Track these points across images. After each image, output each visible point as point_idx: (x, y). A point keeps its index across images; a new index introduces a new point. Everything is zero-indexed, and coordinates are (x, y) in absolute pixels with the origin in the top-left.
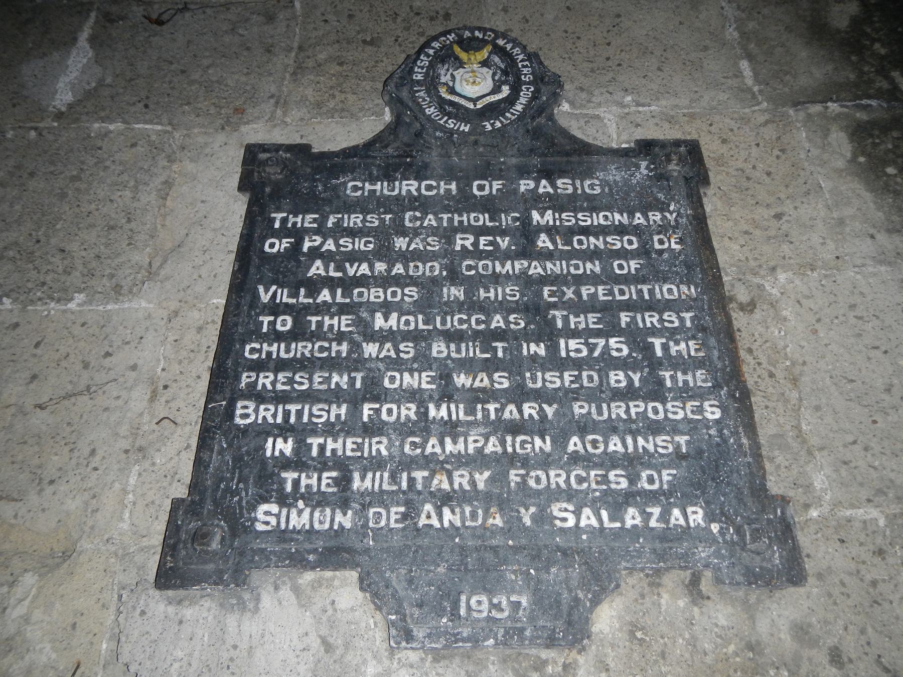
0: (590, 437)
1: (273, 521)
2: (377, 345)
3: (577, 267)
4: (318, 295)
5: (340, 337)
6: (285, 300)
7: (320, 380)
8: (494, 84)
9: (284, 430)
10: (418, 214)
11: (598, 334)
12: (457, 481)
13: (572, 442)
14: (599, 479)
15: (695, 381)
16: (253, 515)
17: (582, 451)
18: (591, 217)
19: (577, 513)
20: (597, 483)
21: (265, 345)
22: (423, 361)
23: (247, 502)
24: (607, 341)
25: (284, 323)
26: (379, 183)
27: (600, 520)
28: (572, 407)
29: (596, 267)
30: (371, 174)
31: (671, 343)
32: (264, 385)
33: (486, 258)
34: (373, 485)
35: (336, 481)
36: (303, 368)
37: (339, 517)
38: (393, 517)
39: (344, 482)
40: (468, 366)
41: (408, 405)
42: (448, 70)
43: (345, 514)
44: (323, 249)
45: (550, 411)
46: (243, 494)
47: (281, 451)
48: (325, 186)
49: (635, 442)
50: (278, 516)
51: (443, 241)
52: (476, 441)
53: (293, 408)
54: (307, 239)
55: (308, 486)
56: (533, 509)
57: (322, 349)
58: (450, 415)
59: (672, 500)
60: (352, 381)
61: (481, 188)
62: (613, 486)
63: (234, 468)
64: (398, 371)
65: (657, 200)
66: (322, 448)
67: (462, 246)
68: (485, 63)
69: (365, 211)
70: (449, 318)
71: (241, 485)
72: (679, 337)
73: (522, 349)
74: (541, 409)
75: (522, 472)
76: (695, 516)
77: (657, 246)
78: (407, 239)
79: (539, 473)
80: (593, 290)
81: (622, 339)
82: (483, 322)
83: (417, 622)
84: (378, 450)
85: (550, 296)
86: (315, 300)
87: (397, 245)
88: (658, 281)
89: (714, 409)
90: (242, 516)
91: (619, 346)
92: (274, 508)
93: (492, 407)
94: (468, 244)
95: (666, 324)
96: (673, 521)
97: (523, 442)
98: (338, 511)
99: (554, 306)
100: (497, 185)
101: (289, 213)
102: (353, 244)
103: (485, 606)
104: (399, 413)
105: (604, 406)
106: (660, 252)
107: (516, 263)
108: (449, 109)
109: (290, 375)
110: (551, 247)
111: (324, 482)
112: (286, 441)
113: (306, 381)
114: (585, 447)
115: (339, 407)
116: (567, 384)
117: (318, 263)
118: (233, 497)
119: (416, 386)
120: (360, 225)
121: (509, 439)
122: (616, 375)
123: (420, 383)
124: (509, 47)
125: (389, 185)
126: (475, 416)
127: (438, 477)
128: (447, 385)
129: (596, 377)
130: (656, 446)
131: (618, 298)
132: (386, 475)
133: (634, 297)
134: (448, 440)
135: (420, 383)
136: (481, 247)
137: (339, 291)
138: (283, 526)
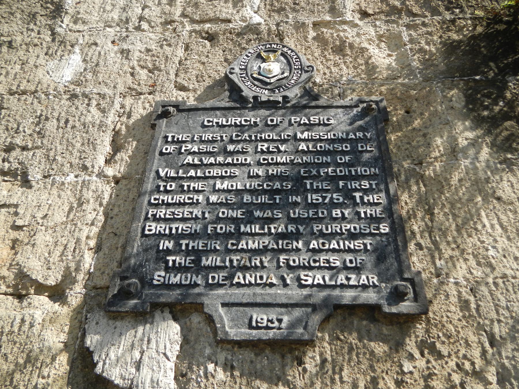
1: (162, 280)
2: (217, 196)
3: (318, 159)
5: (198, 192)
9: (170, 236)
11: (327, 191)
17: (317, 248)
20: (324, 263)
25: (171, 186)
30: (216, 115)
32: (160, 216)
37: (194, 277)
39: (197, 261)
40: (262, 206)
45: (301, 228)
47: (167, 247)
49: (344, 244)
53: (174, 226)
55: (180, 264)
57: (189, 198)
66: (187, 245)
67: (261, 149)
68: (278, 61)
69: (213, 133)
71: (147, 263)
74: (297, 227)
77: (360, 149)
85: (304, 173)
87: (229, 150)
88: (359, 166)
91: (338, 197)
92: (163, 274)
93: (272, 226)
95: (363, 187)
97: (287, 243)
98: (194, 275)
99: (306, 178)
102: (207, 148)
103: (265, 321)
104: (226, 230)
111: (188, 261)
112: (170, 242)
116: (310, 216)
119: (235, 216)
121: (280, 242)
124: (289, 52)
130: (354, 245)
132: (219, 259)
133: (347, 174)
138: (167, 282)
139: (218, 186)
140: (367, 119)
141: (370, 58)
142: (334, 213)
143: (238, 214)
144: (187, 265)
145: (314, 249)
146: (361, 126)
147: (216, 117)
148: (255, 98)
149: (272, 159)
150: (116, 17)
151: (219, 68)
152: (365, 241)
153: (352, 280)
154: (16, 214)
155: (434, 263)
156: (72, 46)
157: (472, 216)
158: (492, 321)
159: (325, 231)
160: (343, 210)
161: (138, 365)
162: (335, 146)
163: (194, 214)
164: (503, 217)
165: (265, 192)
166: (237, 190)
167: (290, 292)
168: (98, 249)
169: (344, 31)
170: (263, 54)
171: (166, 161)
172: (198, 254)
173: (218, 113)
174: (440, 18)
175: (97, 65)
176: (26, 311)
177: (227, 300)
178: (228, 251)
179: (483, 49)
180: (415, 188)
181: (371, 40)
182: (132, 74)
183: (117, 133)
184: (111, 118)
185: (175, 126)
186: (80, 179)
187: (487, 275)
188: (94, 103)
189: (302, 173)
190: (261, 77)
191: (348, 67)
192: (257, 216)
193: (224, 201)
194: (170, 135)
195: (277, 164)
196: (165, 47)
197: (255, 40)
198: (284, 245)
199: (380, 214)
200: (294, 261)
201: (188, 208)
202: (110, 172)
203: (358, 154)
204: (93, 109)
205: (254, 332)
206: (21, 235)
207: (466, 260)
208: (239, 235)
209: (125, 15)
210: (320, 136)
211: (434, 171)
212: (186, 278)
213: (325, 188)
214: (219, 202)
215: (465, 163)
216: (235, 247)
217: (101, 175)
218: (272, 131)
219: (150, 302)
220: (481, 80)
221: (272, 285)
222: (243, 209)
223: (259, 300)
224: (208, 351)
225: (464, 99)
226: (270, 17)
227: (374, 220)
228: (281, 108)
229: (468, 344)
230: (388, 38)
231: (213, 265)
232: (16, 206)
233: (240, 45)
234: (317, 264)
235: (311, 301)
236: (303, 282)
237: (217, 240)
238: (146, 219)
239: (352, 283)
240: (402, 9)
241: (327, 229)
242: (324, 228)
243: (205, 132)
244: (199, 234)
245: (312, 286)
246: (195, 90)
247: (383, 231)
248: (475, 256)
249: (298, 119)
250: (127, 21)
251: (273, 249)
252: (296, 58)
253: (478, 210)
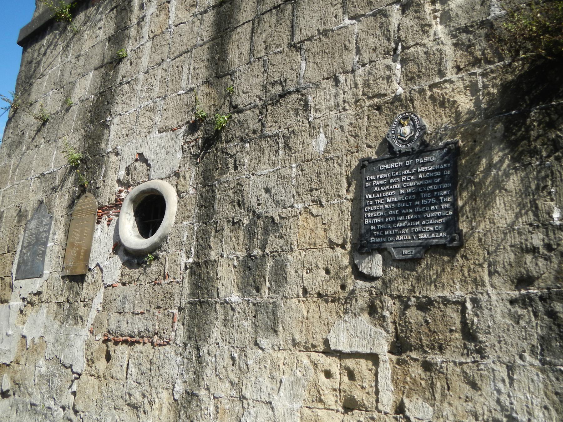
5: (381, 204)
11: (430, 198)
22: (397, 208)
29: (430, 181)
35: (382, 233)
39: (384, 233)
40: (405, 208)
45: (419, 216)
53: (374, 220)
68: (409, 124)
69: (384, 173)
92: (373, 238)
99: (421, 192)
108: (400, 141)
139: (388, 200)
140: (450, 155)
141: (458, 107)
143: (396, 212)
146: (446, 160)
147: (385, 164)
148: (400, 151)
150: (333, 104)
151: (385, 129)
154: (322, 219)
155: (472, 224)
156: (319, 128)
157: (492, 200)
158: (489, 246)
161: (371, 268)
164: (506, 199)
165: (405, 201)
166: (395, 202)
168: (351, 230)
169: (446, 88)
170: (402, 121)
172: (383, 230)
173: (385, 162)
174: (502, 63)
175: (332, 139)
176: (335, 253)
177: (394, 246)
178: (394, 228)
179: (524, 85)
180: (470, 188)
181: (460, 91)
182: (347, 141)
183: (348, 176)
184: (344, 168)
186: (339, 201)
187: (492, 228)
188: (335, 161)
190: (401, 137)
191: (446, 117)
194: (367, 177)
195: (410, 187)
196: (359, 120)
197: (400, 106)
202: (349, 197)
204: (336, 165)
206: (326, 227)
207: (485, 221)
208: (397, 222)
209: (336, 101)
211: (479, 178)
215: (494, 172)
217: (346, 199)
218: (407, 169)
220: (515, 113)
221: (409, 240)
223: (405, 245)
224: (390, 263)
225: (503, 129)
226: (406, 85)
227: (447, 209)
228: (411, 155)
229: (479, 255)
230: (470, 87)
232: (321, 215)
233: (393, 111)
235: (422, 244)
238: (365, 218)
240: (481, 59)
243: (381, 174)
245: (423, 239)
246: (375, 147)
248: (489, 219)
250: (338, 106)
253: (495, 197)
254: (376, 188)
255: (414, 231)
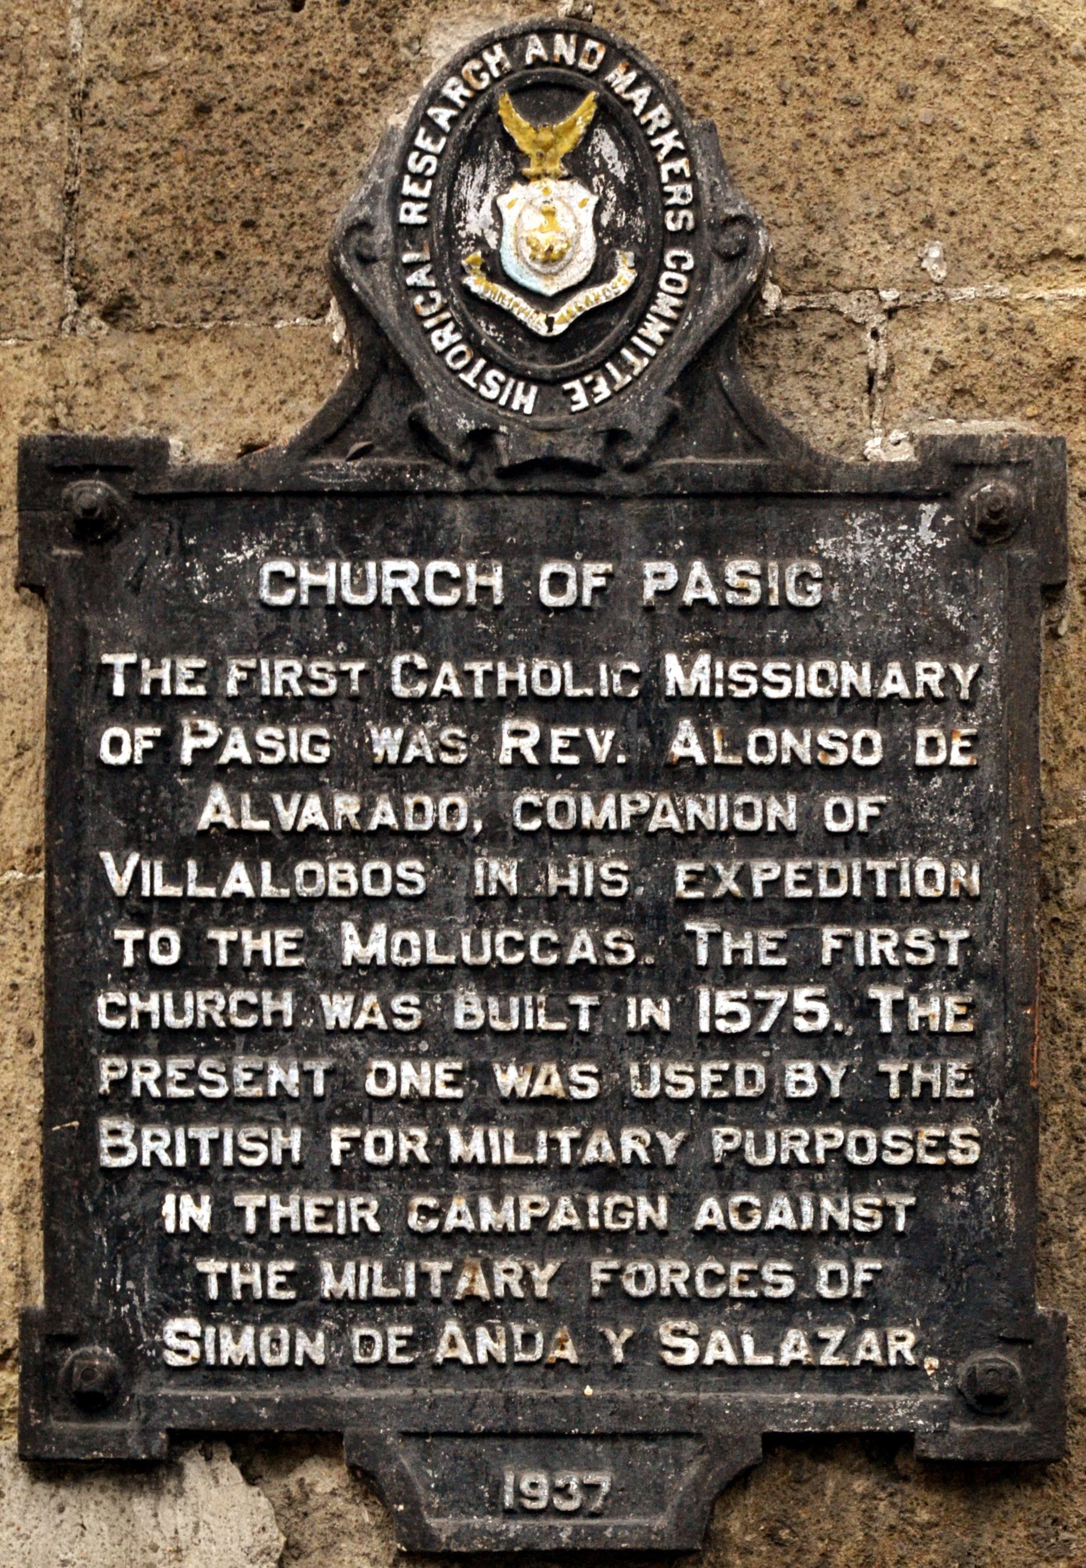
0: (737, 1199)
1: (195, 1350)
3: (748, 810)
4: (225, 878)
6: (159, 891)
7: (248, 1076)
8: (599, 240)
10: (421, 663)
11: (774, 976)
12: (500, 1279)
13: (704, 1210)
14: (746, 1278)
15: (944, 1086)
16: (157, 1338)
17: (722, 1227)
18: (791, 674)
19: (702, 1338)
20: (742, 1285)
21: (134, 998)
23: (144, 1315)
24: (790, 996)
26: (332, 566)
27: (739, 1351)
28: (711, 1139)
31: (913, 1001)
33: (562, 786)
34: (357, 1288)
35: (291, 1279)
36: (212, 1049)
37: (303, 1344)
38: (394, 1344)
41: (413, 1131)
42: (485, 187)
43: (313, 1339)
44: (224, 759)
45: (669, 1145)
46: (136, 1299)
48: (210, 570)
49: (817, 1209)
50: (200, 1340)
51: (475, 738)
52: (534, 1205)
53: (205, 1134)
54: (187, 731)
55: (246, 1288)
56: (627, 1333)
57: (245, 1007)
58: (488, 1153)
59: (866, 1317)
60: (307, 1075)
61: (558, 582)
62: (770, 1292)
63: (112, 1249)
64: (390, 1056)
65: (944, 623)
66: (263, 1213)
69: (307, 650)
70: (486, 938)
72: (931, 986)
73: (626, 1013)
74: (653, 1137)
75: (614, 1264)
76: (900, 1346)
77: (922, 758)
78: (399, 733)
79: (643, 1266)
80: (774, 875)
81: (821, 991)
82: (555, 947)
83: (439, 1514)
84: (362, 1222)
85: (689, 885)
86: (220, 888)
87: (379, 751)
88: (911, 848)
89: (969, 1144)
90: (139, 1340)
92: (192, 1326)
93: (565, 1136)
94: (526, 745)
96: (861, 1355)
97: (619, 1207)
98: (300, 1333)
99: (693, 908)
100: (594, 575)
101: (143, 650)
102: (286, 742)
103: (544, 1492)
104: (396, 1149)
105: (770, 1136)
106: (928, 771)
107: (625, 799)
109: (188, 1063)
110: (701, 760)
111: (273, 1280)
112: (197, 1202)
113: (222, 1080)
114: (727, 1220)
115: (286, 1134)
116: (705, 1093)
117: (218, 795)
118: (119, 1305)
119: (425, 1091)
120: (298, 692)
121: (593, 1201)
122: (799, 1071)
123: (433, 1087)
125: (353, 571)
126: (535, 1153)
127: (467, 1274)
128: (482, 1090)
129: (761, 1078)
130: (852, 1215)
131: (827, 892)
132: (378, 1269)
134: (485, 1203)
135: (433, 1087)
136: (555, 758)
137: (266, 867)
138: (211, 1359)
139: (352, 948)
142: (792, 1077)
144: (272, 1293)
145: (710, 1229)
149: (561, 807)
152: (892, 1202)
153: (831, 1348)
159: (752, 1159)
160: (826, 1068)
162: (824, 741)
163: (273, 1080)
167: (624, 1393)
171: (121, 808)
185: (131, 598)
189: (680, 887)
192: (506, 1092)
193: (380, 1021)
198: (608, 1215)
199: (960, 1084)
200: (640, 1276)
201: (247, 1050)
203: (913, 782)
205: (515, 1527)
210: (762, 681)
212: (276, 1340)
213: (765, 961)
214: (359, 1025)
216: (433, 1224)
218: (561, 653)
219: (169, 1431)
222: (454, 1055)
231: (363, 1294)
234: (719, 1290)
236: (669, 1357)
237: (365, 1190)
239: (827, 1359)
241: (761, 1150)
242: (749, 1147)
243: (269, 646)
244: (299, 1166)
247: (958, 1158)
249: (671, 581)
251: (566, 1229)
252: (674, 154)
254: (218, 795)
255: (613, 1285)
